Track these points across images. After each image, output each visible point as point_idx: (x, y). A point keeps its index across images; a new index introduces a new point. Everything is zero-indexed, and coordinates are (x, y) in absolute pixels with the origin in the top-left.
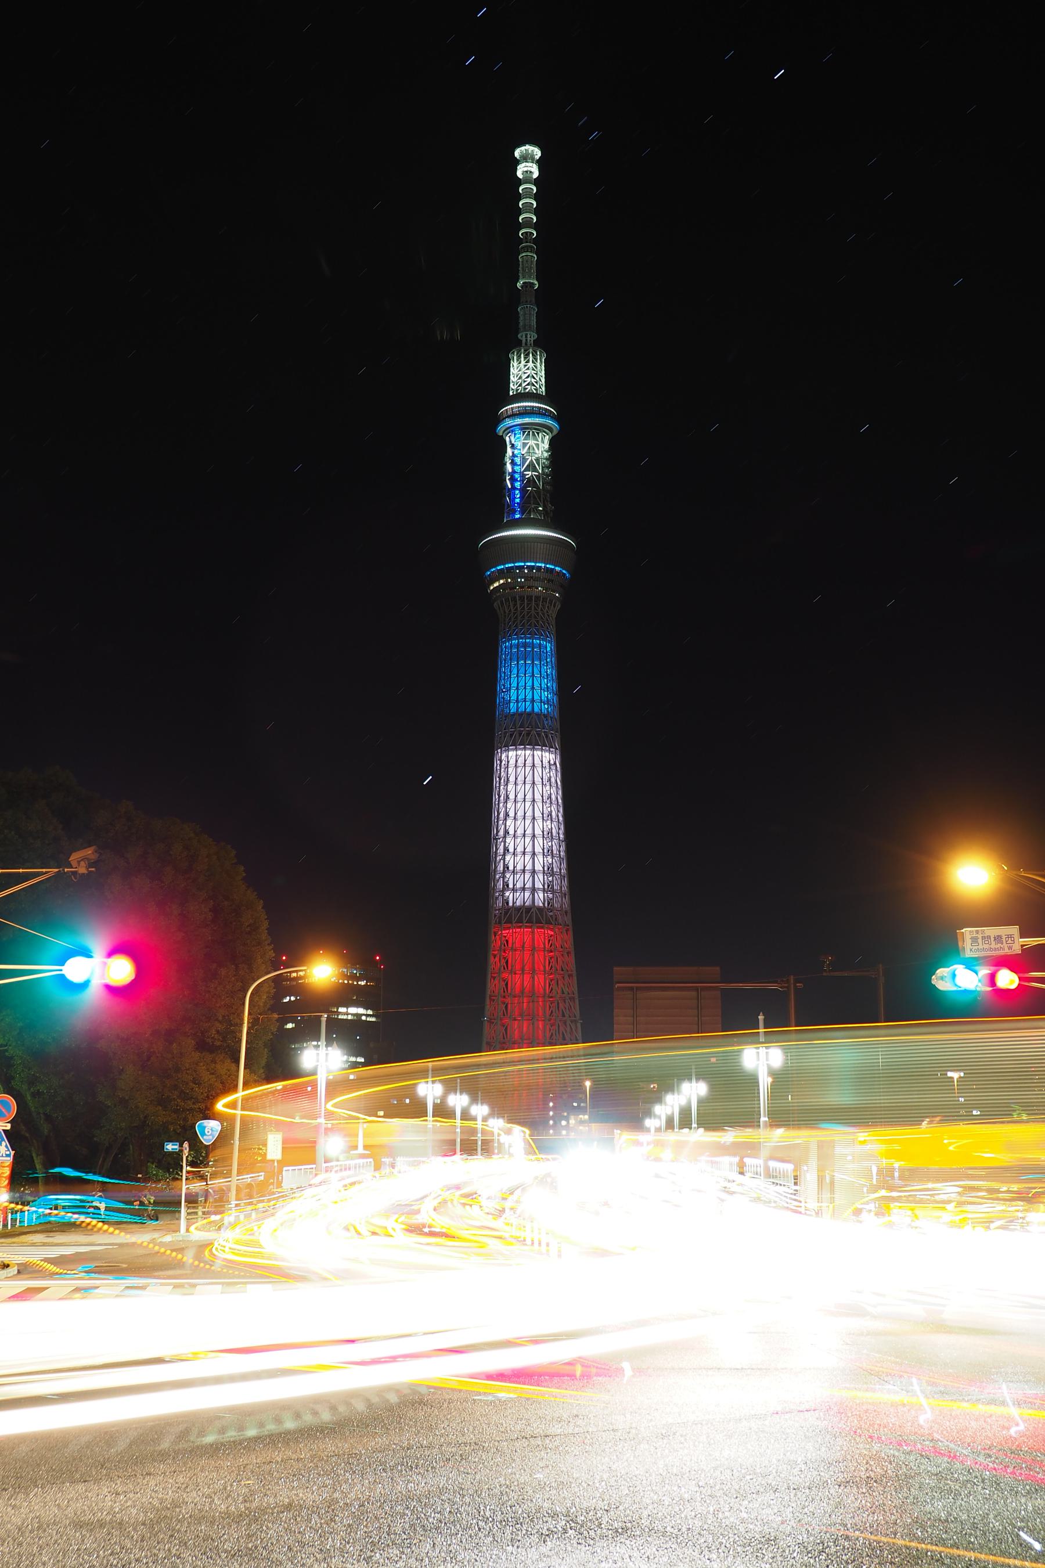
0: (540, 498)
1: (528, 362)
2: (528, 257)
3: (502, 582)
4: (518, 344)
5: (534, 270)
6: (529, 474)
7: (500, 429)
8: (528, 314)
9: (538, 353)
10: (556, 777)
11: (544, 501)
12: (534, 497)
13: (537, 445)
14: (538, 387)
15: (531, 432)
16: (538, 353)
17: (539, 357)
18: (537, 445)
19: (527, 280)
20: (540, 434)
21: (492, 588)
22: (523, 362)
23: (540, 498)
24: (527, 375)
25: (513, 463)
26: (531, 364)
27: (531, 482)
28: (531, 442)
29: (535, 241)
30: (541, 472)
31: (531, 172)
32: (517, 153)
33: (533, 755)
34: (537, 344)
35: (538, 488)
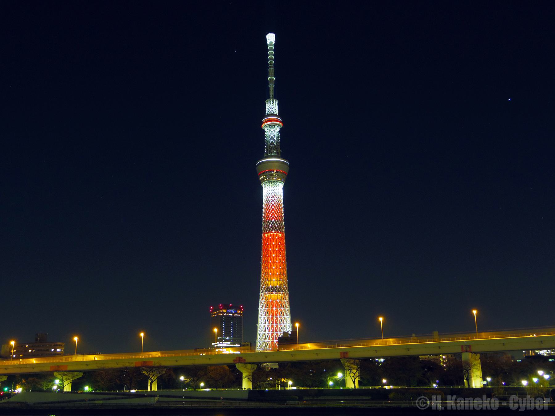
0: (275, 148)
1: (271, 104)
2: (271, 70)
6: (271, 141)
7: (263, 125)
9: (274, 100)
11: (277, 149)
12: (273, 148)
13: (274, 131)
14: (274, 111)
15: (272, 127)
16: (274, 100)
17: (274, 102)
18: (274, 131)
19: (271, 78)
20: (275, 127)
21: (261, 178)
22: (269, 104)
23: (275, 148)
24: (270, 108)
26: (272, 104)
28: (272, 130)
30: (275, 139)
34: (275, 97)
35: (274, 145)
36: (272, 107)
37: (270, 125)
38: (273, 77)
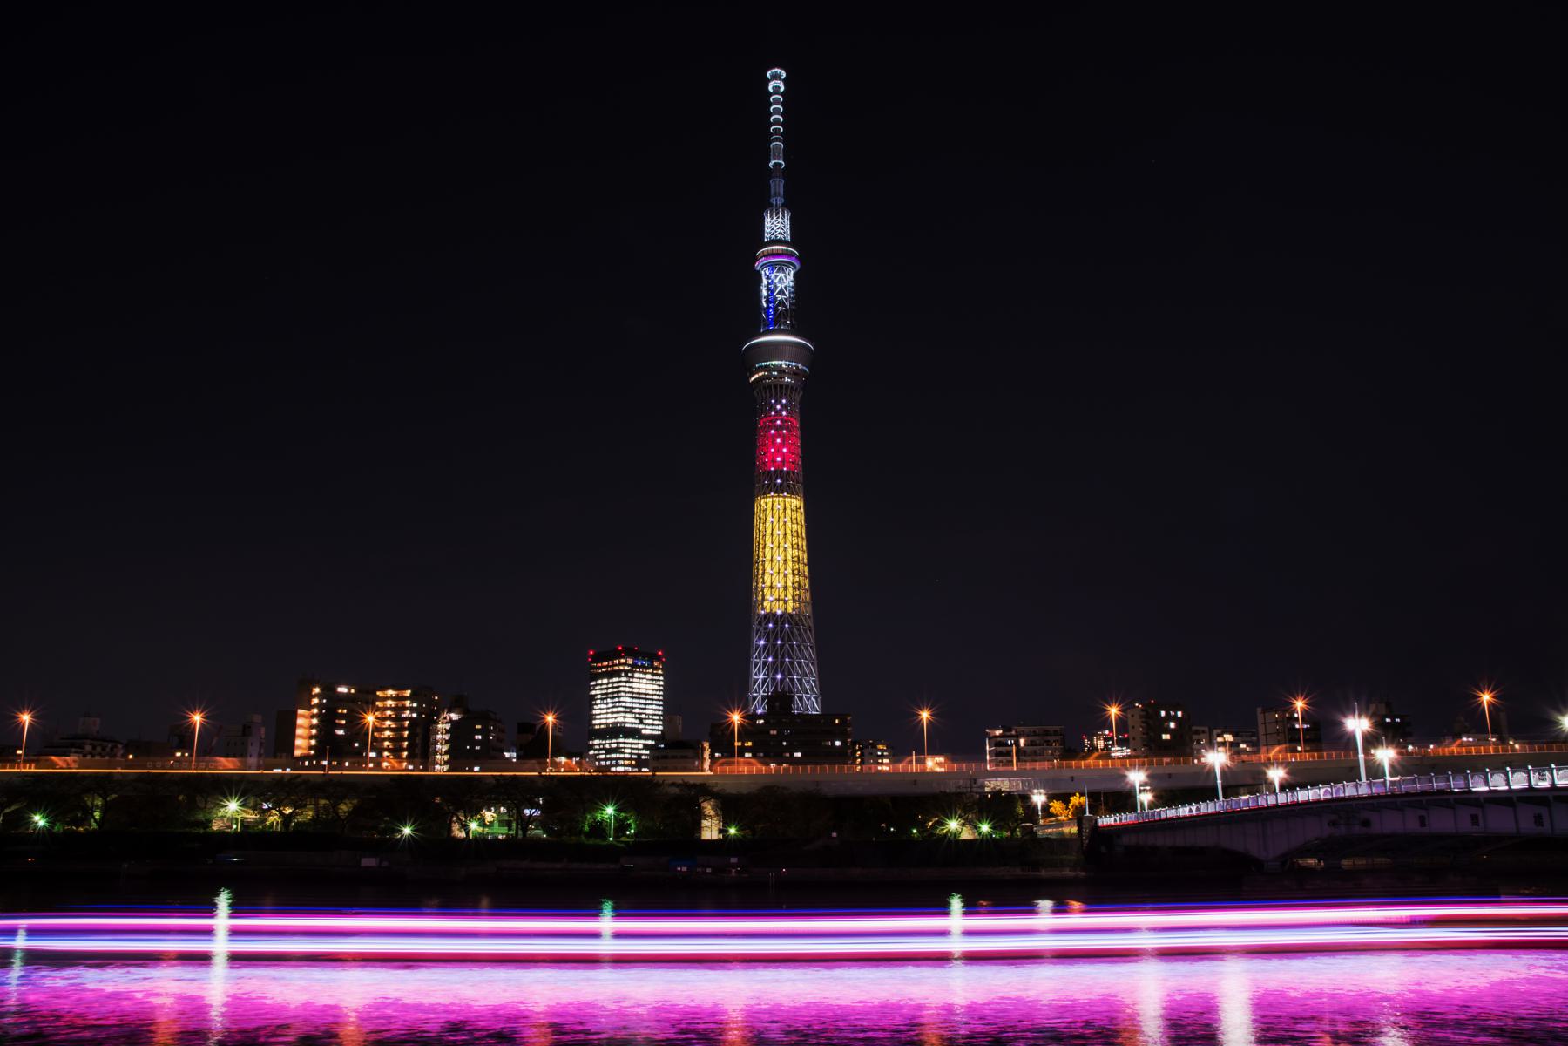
1: (772, 218)
2: (777, 145)
3: (760, 374)
4: (770, 206)
5: (781, 155)
7: (758, 265)
8: (778, 186)
10: (800, 517)
25: (768, 289)
27: (781, 303)
29: (781, 135)
31: (776, 87)
32: (768, 75)
33: (785, 502)
34: (784, 205)
35: (786, 307)
36: (776, 225)
37: (771, 266)
38: (779, 159)
